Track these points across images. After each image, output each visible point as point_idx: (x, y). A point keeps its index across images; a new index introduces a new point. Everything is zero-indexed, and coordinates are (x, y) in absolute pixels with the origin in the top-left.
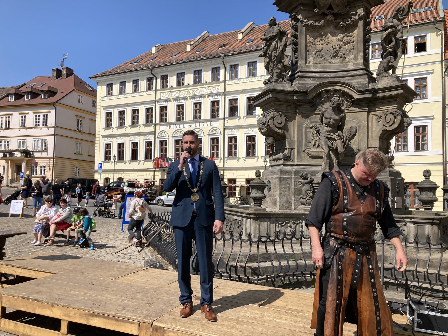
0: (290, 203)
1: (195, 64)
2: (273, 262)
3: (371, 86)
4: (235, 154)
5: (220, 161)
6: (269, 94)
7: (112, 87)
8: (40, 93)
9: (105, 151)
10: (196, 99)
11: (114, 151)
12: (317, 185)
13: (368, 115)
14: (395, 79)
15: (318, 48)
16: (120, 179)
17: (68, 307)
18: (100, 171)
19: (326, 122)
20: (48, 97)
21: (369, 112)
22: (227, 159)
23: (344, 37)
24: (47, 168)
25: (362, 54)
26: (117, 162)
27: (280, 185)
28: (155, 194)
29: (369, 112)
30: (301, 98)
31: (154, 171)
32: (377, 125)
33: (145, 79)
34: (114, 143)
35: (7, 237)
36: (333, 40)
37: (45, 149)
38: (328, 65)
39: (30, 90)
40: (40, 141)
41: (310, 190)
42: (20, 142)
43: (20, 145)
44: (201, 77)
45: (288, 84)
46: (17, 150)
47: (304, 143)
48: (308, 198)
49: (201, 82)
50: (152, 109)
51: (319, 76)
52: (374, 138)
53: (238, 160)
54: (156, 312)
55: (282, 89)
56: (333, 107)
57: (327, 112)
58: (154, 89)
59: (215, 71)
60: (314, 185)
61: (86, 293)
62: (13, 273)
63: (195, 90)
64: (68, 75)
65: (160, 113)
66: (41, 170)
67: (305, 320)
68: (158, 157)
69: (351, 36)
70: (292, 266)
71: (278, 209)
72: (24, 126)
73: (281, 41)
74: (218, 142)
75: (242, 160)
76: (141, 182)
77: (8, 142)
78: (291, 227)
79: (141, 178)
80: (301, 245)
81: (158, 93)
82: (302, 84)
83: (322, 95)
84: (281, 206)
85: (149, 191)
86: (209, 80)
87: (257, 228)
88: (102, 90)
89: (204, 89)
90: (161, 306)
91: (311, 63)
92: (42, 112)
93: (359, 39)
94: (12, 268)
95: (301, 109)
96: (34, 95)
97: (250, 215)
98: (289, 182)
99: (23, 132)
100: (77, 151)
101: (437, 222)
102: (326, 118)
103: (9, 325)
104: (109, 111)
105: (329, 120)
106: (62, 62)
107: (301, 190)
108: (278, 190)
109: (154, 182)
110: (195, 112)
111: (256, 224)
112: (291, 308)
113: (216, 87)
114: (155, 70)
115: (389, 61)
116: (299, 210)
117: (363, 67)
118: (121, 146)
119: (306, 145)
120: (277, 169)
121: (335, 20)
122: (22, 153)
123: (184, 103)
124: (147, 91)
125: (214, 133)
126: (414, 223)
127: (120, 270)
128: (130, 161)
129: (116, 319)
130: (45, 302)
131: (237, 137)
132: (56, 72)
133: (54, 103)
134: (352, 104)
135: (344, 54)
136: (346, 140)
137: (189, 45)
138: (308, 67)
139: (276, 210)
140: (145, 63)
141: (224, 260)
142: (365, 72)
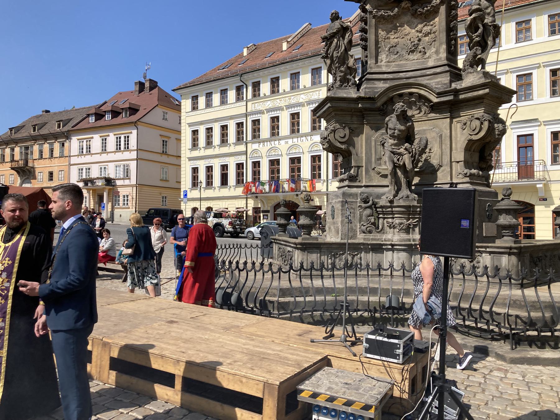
0: (355, 231)
1: (291, 66)
3: (454, 86)
5: (323, 184)
6: (327, 103)
7: (197, 100)
8: (121, 111)
9: (192, 175)
10: (293, 109)
11: (202, 176)
12: (381, 210)
13: (451, 123)
14: (481, 75)
15: (392, 43)
18: (185, 200)
20: (130, 116)
21: (452, 118)
23: (424, 26)
24: (130, 198)
25: (444, 46)
26: (205, 188)
27: (342, 210)
28: (244, 226)
29: (452, 118)
30: (368, 106)
31: (247, 198)
32: (462, 134)
33: (235, 88)
34: (202, 166)
36: (409, 32)
38: (404, 62)
39: (110, 109)
40: (122, 167)
41: (372, 216)
42: (101, 168)
43: (101, 172)
44: (298, 82)
45: (353, 89)
46: (98, 178)
48: (369, 225)
49: (299, 87)
50: (242, 123)
51: (392, 77)
52: (459, 150)
55: (345, 96)
57: (390, 121)
58: (245, 99)
60: (378, 210)
63: (292, 97)
64: (151, 89)
65: (252, 128)
66: (124, 200)
69: (432, 25)
72: (105, 150)
73: (344, 39)
74: (320, 161)
77: (89, 169)
79: (232, 207)
82: (370, 88)
83: (394, 100)
85: (238, 222)
88: (186, 104)
89: (302, 96)
90: (125, 327)
91: (384, 62)
92: (123, 133)
93: (441, 28)
95: (369, 118)
98: (353, 207)
99: (104, 157)
100: (163, 177)
101: (515, 251)
102: (390, 129)
104: (195, 128)
105: (393, 131)
106: (145, 74)
108: (340, 216)
111: (303, 255)
113: (317, 92)
114: (245, 77)
115: (475, 53)
117: (445, 62)
118: (209, 169)
119: (375, 162)
121: (411, 7)
124: (236, 102)
126: (490, 253)
128: (220, 188)
132: (138, 86)
133: (136, 122)
134: (432, 110)
135: (424, 48)
136: (416, 154)
137: (286, 43)
138: (380, 67)
139: (338, 240)
140: (235, 68)
142: (447, 68)
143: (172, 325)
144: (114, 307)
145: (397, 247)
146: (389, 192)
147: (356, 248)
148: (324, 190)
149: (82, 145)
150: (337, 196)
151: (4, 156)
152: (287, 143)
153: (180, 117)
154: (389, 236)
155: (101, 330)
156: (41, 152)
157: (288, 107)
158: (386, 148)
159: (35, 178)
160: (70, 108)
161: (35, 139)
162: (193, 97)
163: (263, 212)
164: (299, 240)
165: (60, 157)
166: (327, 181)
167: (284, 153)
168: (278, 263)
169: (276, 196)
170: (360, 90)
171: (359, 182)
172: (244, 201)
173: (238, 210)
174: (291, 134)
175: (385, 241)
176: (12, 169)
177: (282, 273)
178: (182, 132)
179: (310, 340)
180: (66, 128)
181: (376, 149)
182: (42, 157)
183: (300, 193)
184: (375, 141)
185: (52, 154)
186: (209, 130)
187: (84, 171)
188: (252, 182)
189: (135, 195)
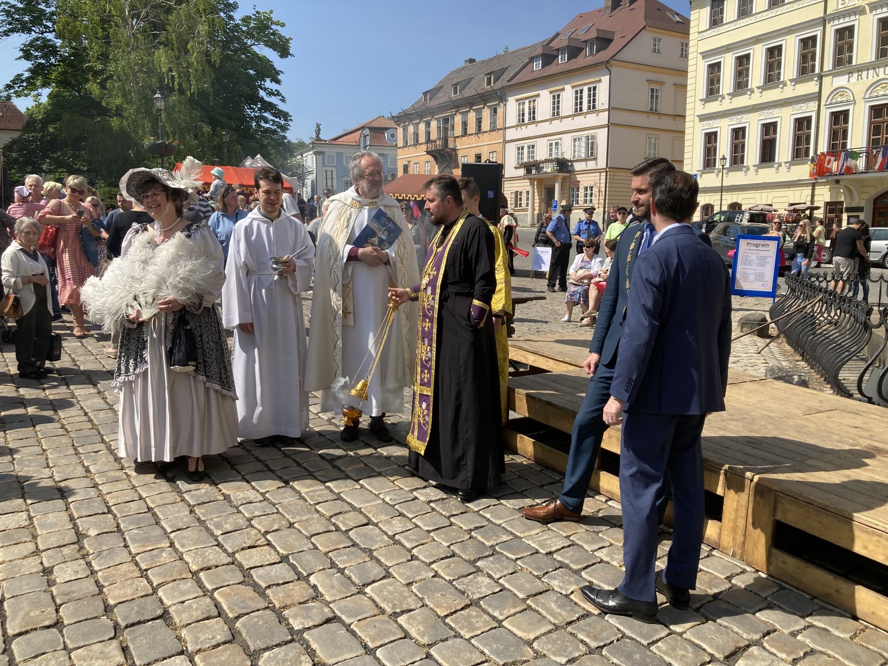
9: (705, 147)
11: (724, 148)
16: (735, 207)
20: (597, 52)
24: (595, 190)
26: (730, 170)
31: (814, 186)
34: (724, 129)
35: (518, 303)
37: (592, 153)
39: (566, 44)
40: (584, 139)
43: (551, 150)
46: (547, 161)
50: (814, 39)
62: (523, 361)
68: (825, 151)
72: (558, 114)
76: (782, 209)
77: (533, 147)
79: (780, 203)
88: (700, 18)
96: (574, 51)
99: (557, 126)
100: (650, 154)
104: (713, 60)
109: (813, 209)
118: (739, 134)
128: (758, 167)
133: (608, 61)
149: (523, 110)
153: (685, 46)
156: (465, 124)
160: (503, 53)
163: (848, 210)
165: (491, 131)
172: (808, 191)
173: (793, 207)
176: (428, 153)
178: (690, 69)
185: (480, 126)
187: (526, 150)
188: (829, 153)
189: (603, 185)
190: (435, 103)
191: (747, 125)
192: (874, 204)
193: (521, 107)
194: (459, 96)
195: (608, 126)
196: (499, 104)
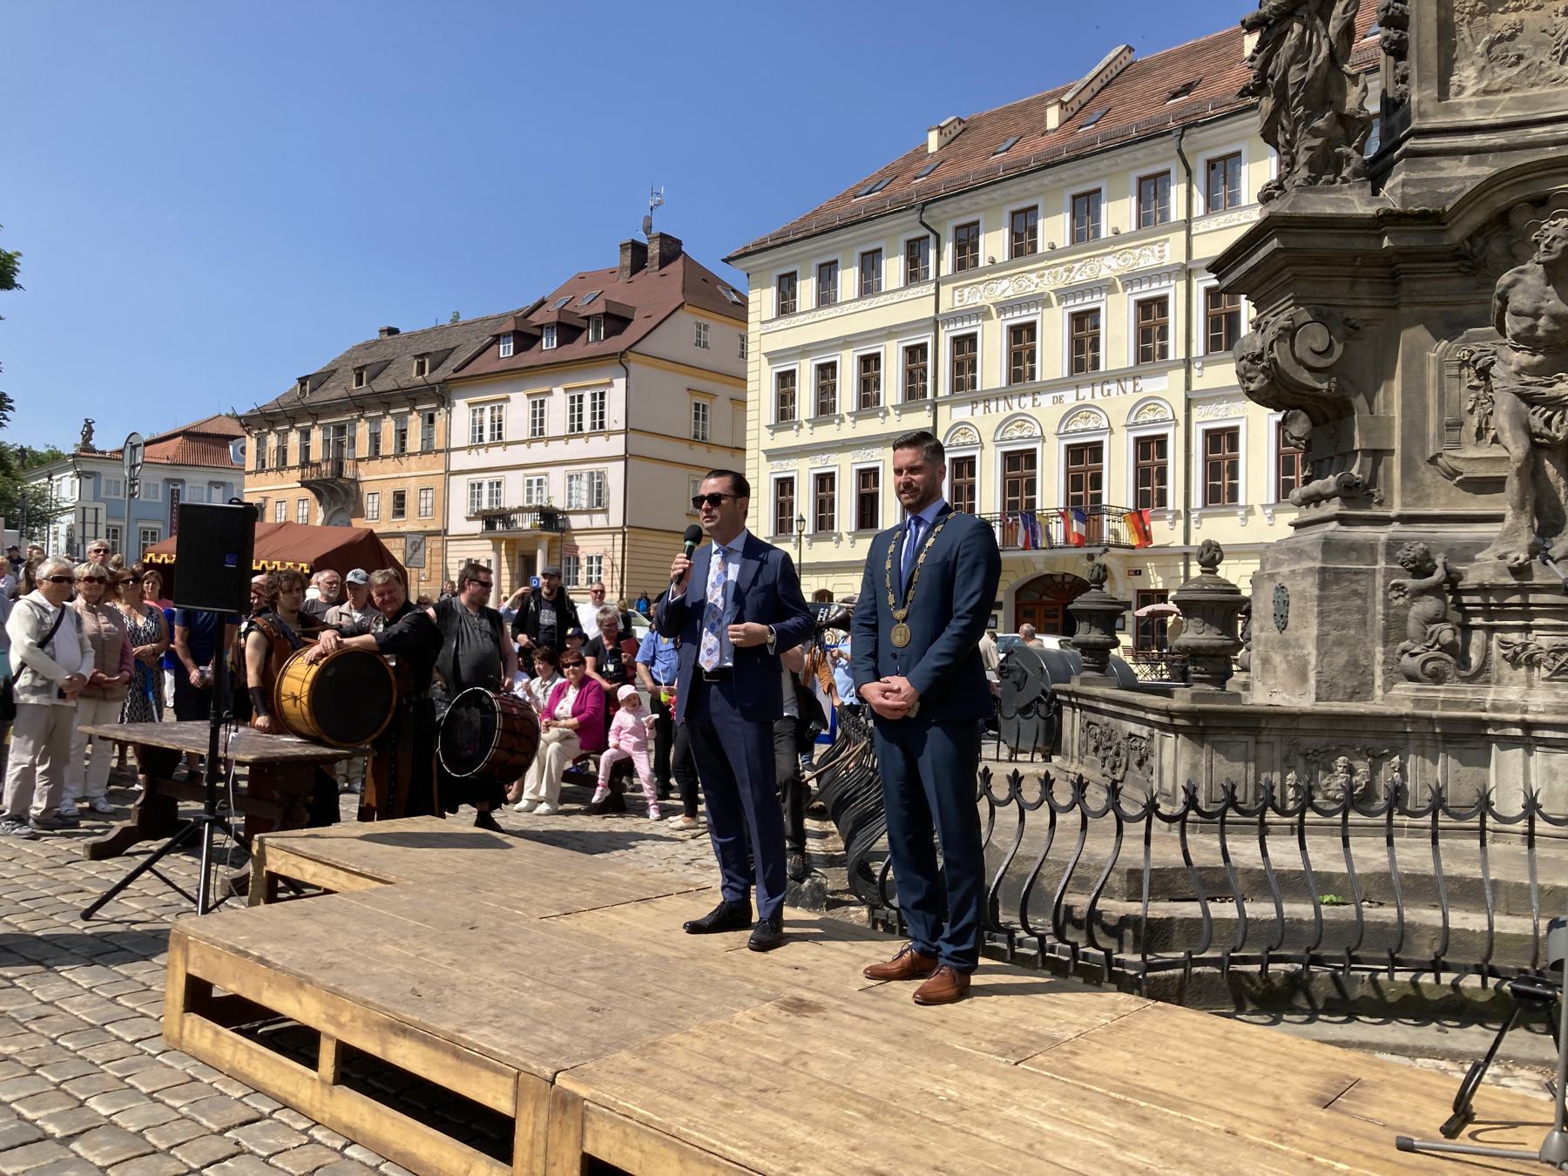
0: (1367, 672)
2: (1246, 906)
4: (1233, 496)
5: (1173, 523)
8: (583, 324)
9: (777, 501)
10: (1079, 301)
11: (804, 503)
12: (1477, 599)
17: (335, 992)
19: (1518, 329)
20: (606, 337)
22: (1201, 516)
24: (606, 563)
26: (813, 539)
27: (1321, 599)
30: (1414, 241)
33: (902, 247)
34: (803, 473)
37: (599, 503)
39: (554, 318)
40: (585, 477)
41: (1444, 620)
42: (530, 483)
43: (530, 491)
44: (1097, 218)
45: (1356, 191)
46: (521, 510)
47: (1432, 428)
48: (1432, 653)
53: (1245, 519)
54: (595, 1042)
55: (1329, 210)
56: (1546, 264)
57: (1519, 287)
58: (932, 276)
59: (1151, 190)
60: (1465, 599)
61: (423, 954)
64: (665, 260)
65: (953, 361)
66: (590, 571)
67: (1173, 1144)
70: (1332, 923)
71: (1313, 696)
72: (541, 432)
74: (1162, 453)
75: (1260, 518)
77: (498, 484)
78: (1351, 770)
80: (1390, 843)
81: (945, 290)
83: (1514, 219)
84: (1324, 686)
86: (1128, 224)
87: (1203, 769)
88: (762, 301)
89: (1108, 260)
90: (631, 1021)
94: (294, 859)
95: (1419, 286)
96: (568, 331)
97: (1172, 717)
98: (1361, 589)
99: (539, 452)
102: (1517, 313)
103: (202, 1036)
105: (1529, 321)
106: (648, 219)
107: (1405, 620)
108: (1314, 621)
110: (1077, 346)
112: (1152, 1085)
113: (1156, 248)
114: (935, 210)
116: (1391, 701)
118: (825, 482)
119: (1440, 436)
120: (1317, 533)
122: (536, 516)
123: (1038, 318)
124: (907, 285)
125: (1150, 418)
127: (605, 886)
128: (854, 536)
129: (454, 1049)
130: (283, 970)
131: (1236, 428)
132: (629, 253)
133: (622, 353)
139: (1303, 700)
141: (1045, 882)
143: (802, 1021)
144: (587, 923)
145: (1548, 734)
146: (1503, 538)
147: (1385, 736)
148: (1180, 542)
149: (481, 422)
150: (1293, 551)
151: (285, 451)
152: (1060, 400)
154: (1512, 694)
155: (542, 1032)
156: (375, 439)
157: (1065, 294)
158: (1495, 383)
159: (360, 512)
160: (447, 323)
161: (359, 405)
162: (781, 277)
164: (1181, 699)
165: (422, 453)
166: (1187, 513)
167: (1050, 430)
168: (1083, 770)
169: (1023, 561)
170: (1383, 192)
171: (1380, 503)
174: (1071, 373)
175: (1495, 708)
176: (304, 484)
177: (1155, 820)
179: (1391, 1136)
180: (440, 375)
181: (1441, 389)
182: (377, 453)
183: (1100, 550)
184: (1441, 365)
185: (403, 444)
186: (827, 372)
187: (486, 489)
190: (321, 397)
191: (836, 470)
192: (1017, 598)
193: (478, 416)
194: (365, 388)
195: (625, 458)
196: (438, 409)
